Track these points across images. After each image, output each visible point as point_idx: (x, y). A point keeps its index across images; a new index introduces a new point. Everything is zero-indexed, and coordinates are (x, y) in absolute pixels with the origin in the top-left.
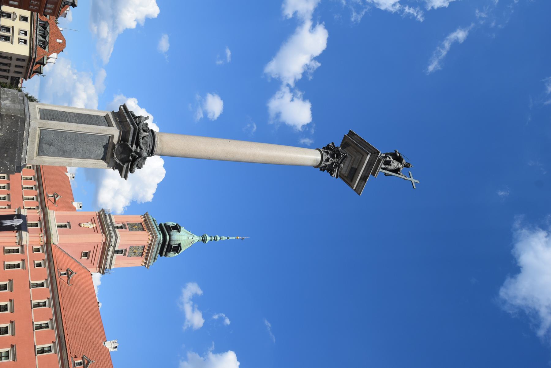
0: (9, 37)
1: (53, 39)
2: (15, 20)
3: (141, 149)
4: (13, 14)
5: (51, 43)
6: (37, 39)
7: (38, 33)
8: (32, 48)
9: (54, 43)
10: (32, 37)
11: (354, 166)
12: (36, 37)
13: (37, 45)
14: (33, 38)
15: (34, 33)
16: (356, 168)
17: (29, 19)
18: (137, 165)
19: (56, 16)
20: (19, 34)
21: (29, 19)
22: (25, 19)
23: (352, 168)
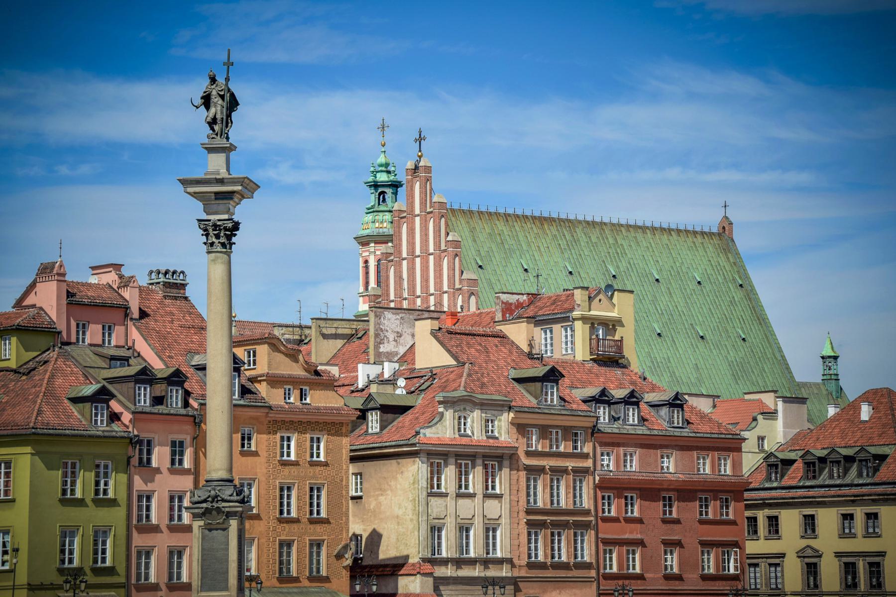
0: (871, 564)
1: (859, 434)
2: (817, 551)
3: (209, 497)
4: (804, 557)
5: (870, 438)
6: (856, 482)
7: (838, 482)
8: (881, 497)
9: (871, 428)
10: (853, 498)
11: (213, 197)
12: (851, 485)
13: (876, 479)
14: (855, 496)
15: (840, 492)
16: (213, 194)
17: (809, 511)
18: (230, 496)
19: (740, 441)
20: (854, 536)
21: (809, 511)
22: (810, 522)
23: (216, 199)
